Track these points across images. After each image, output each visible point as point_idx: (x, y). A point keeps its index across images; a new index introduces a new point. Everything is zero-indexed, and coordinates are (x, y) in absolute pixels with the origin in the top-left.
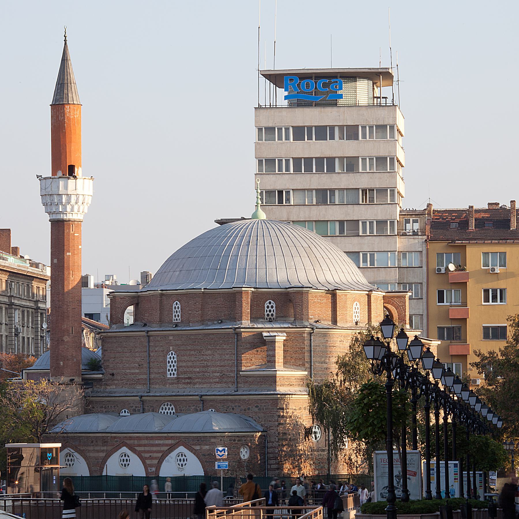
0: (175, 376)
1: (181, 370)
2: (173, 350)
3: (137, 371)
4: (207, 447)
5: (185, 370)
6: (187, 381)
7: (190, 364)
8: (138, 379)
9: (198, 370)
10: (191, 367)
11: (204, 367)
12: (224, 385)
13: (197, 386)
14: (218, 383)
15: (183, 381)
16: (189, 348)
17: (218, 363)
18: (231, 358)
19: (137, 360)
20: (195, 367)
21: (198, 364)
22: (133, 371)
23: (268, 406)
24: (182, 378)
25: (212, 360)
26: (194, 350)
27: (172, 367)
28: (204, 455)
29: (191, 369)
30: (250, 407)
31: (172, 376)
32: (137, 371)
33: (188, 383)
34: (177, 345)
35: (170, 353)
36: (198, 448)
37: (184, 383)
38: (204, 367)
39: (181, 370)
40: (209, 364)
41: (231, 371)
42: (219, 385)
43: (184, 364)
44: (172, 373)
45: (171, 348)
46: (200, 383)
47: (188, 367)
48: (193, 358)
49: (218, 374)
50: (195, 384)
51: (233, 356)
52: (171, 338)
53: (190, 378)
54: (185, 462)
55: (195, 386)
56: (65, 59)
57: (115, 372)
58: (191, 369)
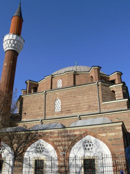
0: (60, 110)
1: (63, 107)
2: (59, 98)
3: (38, 111)
4: (113, 134)
5: (66, 107)
6: (67, 112)
7: (69, 103)
8: (38, 114)
9: (74, 106)
10: (69, 105)
11: (77, 104)
12: (91, 111)
13: (74, 113)
14: (87, 110)
15: (65, 112)
16: (68, 96)
17: (87, 101)
18: (95, 97)
19: (39, 105)
20: (72, 105)
21: (74, 103)
22: (36, 111)
23: (126, 117)
24: (64, 111)
25: (82, 100)
26: (71, 97)
27: (58, 105)
28: (110, 140)
29: (69, 106)
30: (113, 119)
31: (58, 111)
32: (38, 111)
33: (67, 113)
34: (61, 96)
35: (57, 100)
36: (104, 135)
37: (66, 113)
38: (77, 104)
39: (63, 107)
40: (80, 102)
41: (95, 104)
42: (88, 112)
43: (65, 104)
44: (58, 109)
45: (58, 98)
46: (75, 112)
47: (68, 105)
48: (71, 101)
49: (87, 106)
50: (72, 113)
51: (96, 96)
52: (58, 93)
53: (68, 110)
54: (92, 147)
55: (72, 114)
56: (20, 8)
57: (26, 112)
58: (69, 106)
